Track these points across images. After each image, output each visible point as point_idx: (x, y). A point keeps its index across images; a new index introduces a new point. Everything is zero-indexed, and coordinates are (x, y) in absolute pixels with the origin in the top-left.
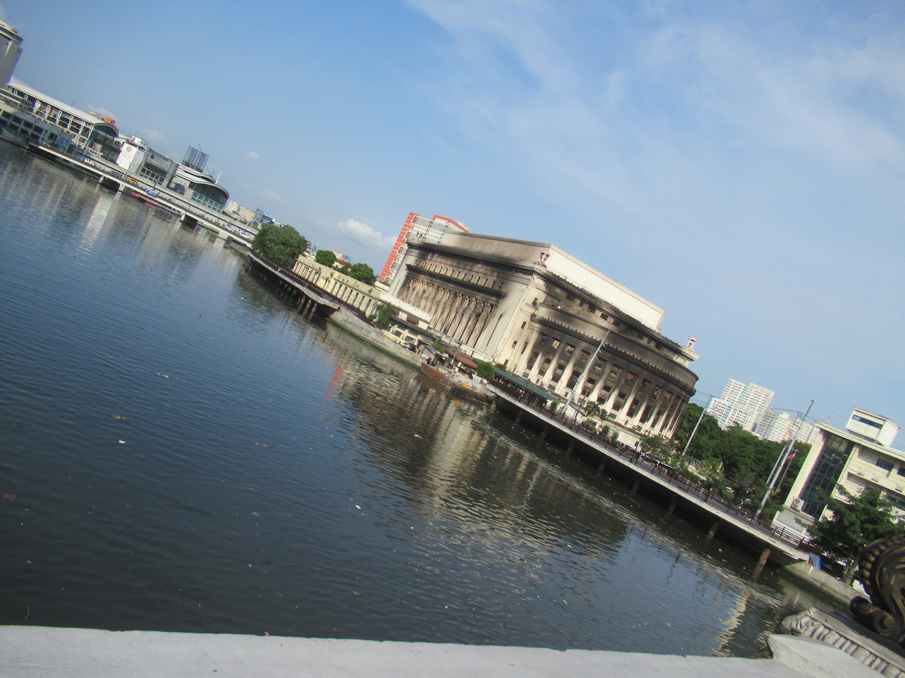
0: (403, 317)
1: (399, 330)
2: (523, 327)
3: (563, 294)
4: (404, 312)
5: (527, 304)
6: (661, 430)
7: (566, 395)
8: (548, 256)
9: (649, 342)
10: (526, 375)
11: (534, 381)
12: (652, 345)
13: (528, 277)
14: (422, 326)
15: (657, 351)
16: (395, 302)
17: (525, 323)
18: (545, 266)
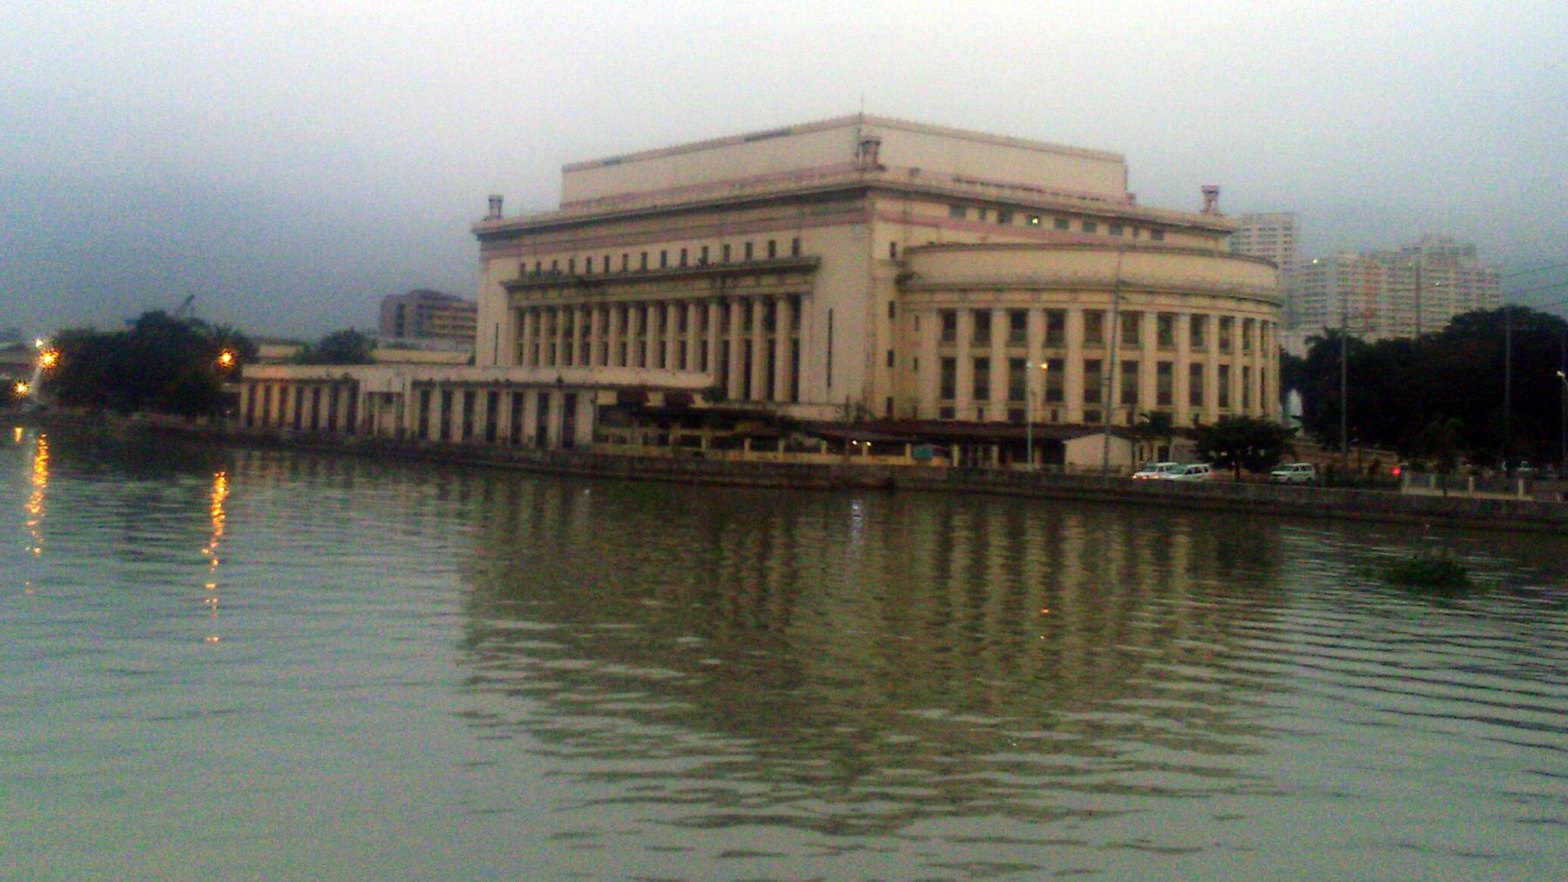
0: (655, 400)
1: (687, 432)
2: (892, 313)
3: (942, 211)
4: (656, 389)
5: (883, 263)
6: (1263, 406)
7: (1055, 416)
8: (878, 144)
9: (1135, 235)
10: (948, 412)
11: (972, 417)
12: (1145, 236)
13: (859, 204)
14: (699, 403)
15: (1157, 243)
16: (628, 376)
17: (892, 306)
18: (882, 168)
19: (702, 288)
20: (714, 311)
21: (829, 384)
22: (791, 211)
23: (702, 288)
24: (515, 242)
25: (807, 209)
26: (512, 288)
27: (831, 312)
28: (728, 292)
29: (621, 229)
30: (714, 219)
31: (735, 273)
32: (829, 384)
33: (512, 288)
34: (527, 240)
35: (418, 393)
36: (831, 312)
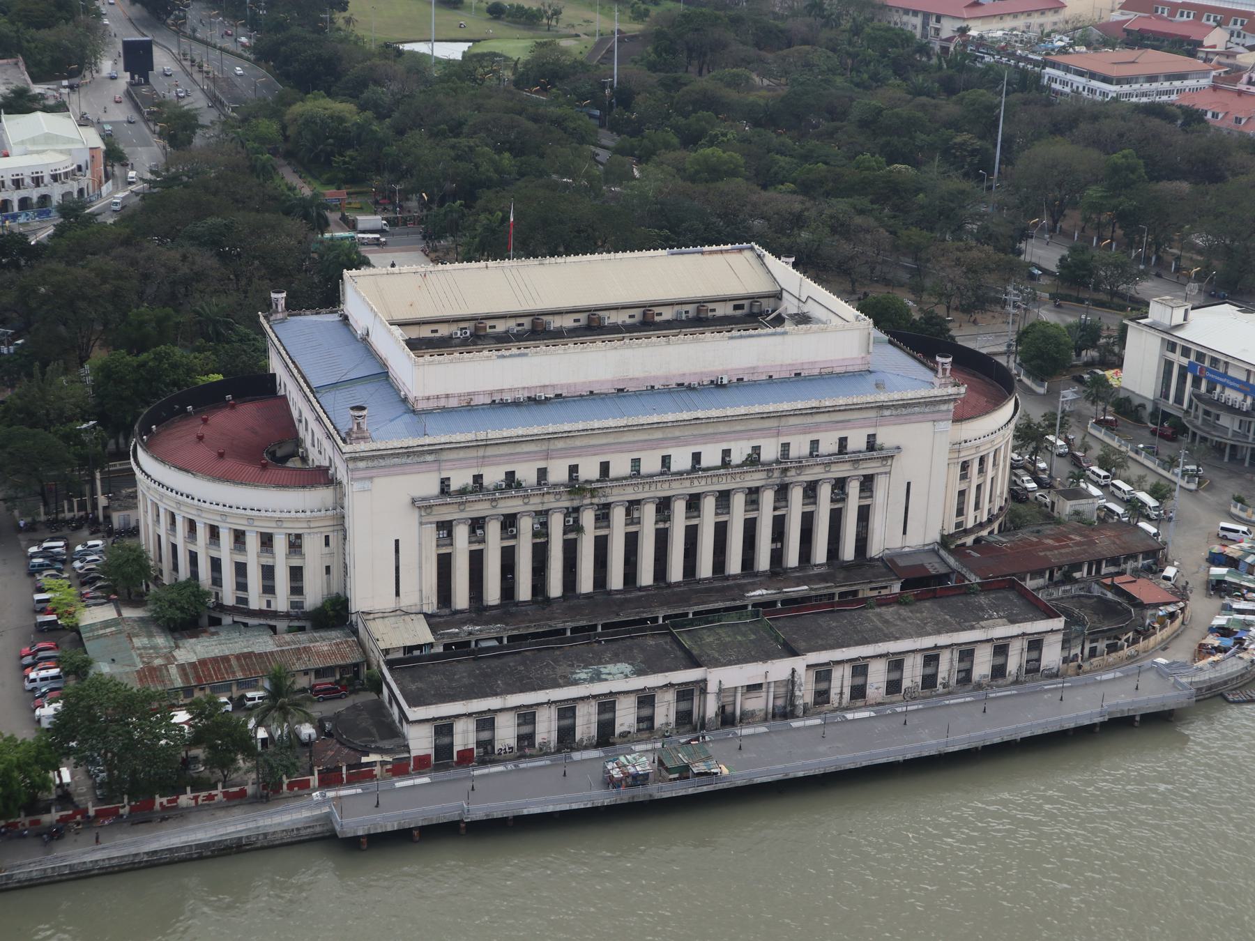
19: (755, 479)
20: (768, 498)
21: (904, 533)
22: (872, 414)
23: (755, 479)
24: (429, 458)
25: (887, 413)
26: (421, 505)
27: (909, 484)
28: (787, 480)
29: (629, 437)
30: (772, 423)
31: (800, 465)
32: (904, 533)
33: (421, 505)
34: (445, 456)
35: (812, 674)
36: (909, 484)
